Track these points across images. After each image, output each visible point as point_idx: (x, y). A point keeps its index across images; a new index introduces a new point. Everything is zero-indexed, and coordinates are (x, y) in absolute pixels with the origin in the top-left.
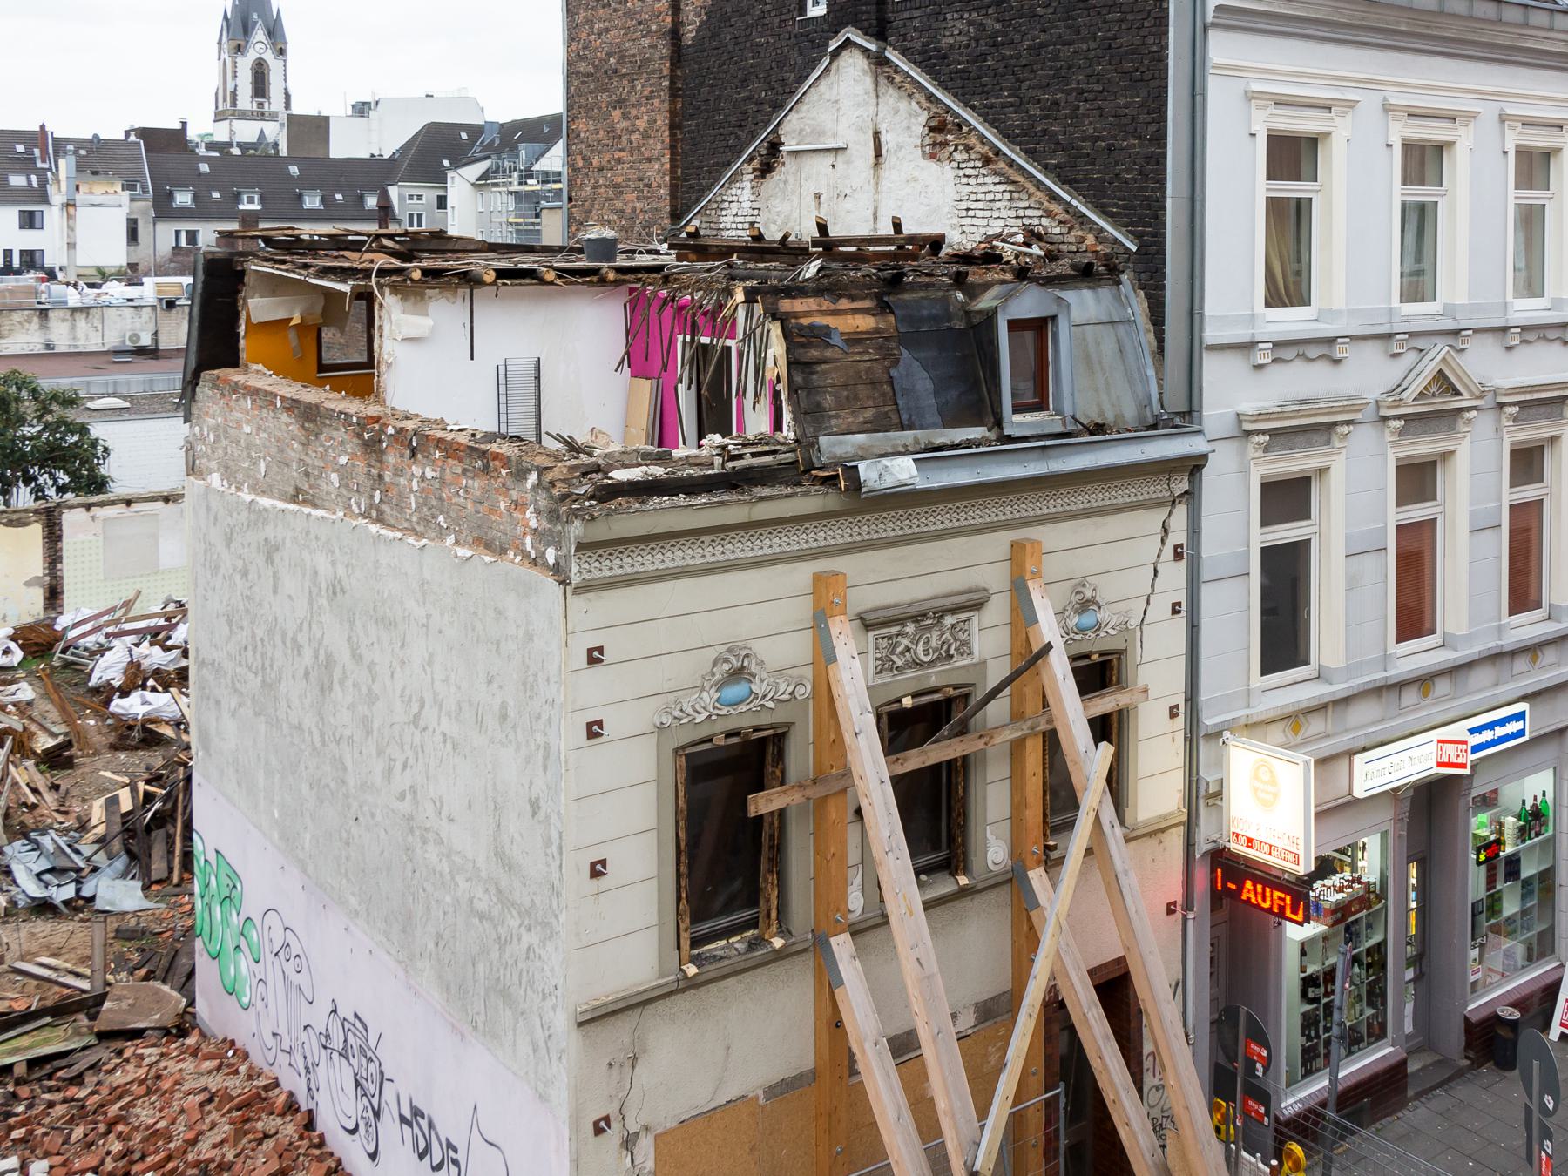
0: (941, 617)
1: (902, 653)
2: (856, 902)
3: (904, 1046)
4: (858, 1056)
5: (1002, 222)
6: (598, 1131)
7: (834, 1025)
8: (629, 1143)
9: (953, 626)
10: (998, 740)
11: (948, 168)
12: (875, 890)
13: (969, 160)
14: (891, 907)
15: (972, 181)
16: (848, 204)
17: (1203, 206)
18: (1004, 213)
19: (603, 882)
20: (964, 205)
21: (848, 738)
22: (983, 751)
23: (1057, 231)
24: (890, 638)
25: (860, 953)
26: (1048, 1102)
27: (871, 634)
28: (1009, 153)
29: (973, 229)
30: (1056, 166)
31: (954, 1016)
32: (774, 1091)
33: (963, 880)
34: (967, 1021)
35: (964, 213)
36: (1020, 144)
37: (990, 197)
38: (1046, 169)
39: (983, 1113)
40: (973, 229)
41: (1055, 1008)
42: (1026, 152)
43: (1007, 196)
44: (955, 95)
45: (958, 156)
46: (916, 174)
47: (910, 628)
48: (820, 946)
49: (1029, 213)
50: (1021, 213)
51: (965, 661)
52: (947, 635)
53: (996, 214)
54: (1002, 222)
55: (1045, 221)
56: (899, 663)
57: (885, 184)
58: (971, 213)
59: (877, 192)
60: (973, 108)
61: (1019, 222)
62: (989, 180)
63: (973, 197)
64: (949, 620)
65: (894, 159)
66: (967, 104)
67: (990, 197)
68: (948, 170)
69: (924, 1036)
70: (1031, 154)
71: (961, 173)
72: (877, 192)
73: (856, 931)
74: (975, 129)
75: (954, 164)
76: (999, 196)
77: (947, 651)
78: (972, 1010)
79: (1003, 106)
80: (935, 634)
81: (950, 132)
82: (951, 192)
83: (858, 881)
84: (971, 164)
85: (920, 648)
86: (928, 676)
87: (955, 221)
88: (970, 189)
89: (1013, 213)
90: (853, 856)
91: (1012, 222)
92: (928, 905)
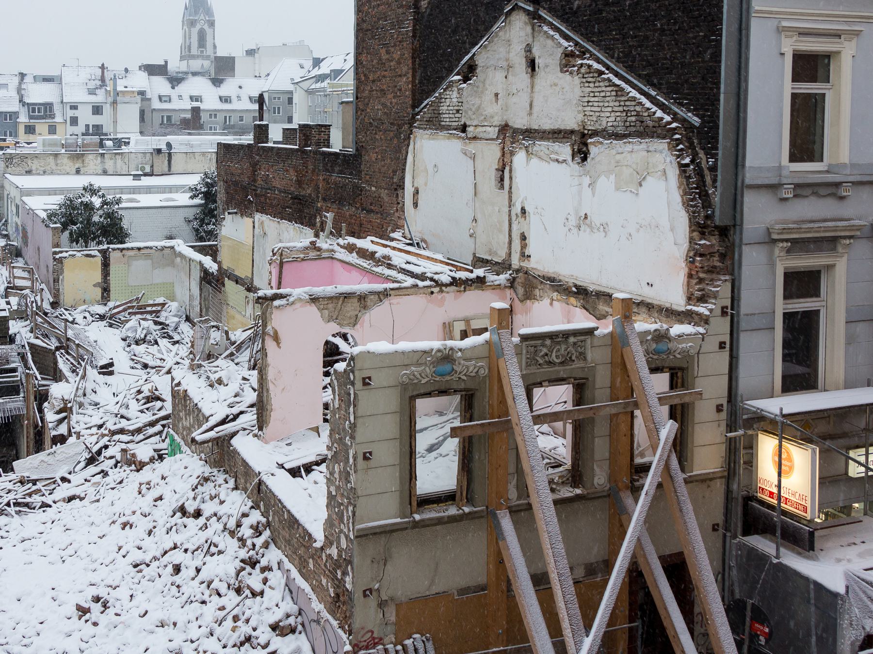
0: (567, 337)
1: (543, 356)
2: (513, 494)
3: (540, 580)
4: (512, 581)
5: (610, 109)
6: (365, 596)
7: (499, 561)
8: (382, 605)
9: (575, 344)
10: (602, 413)
11: (576, 78)
12: (523, 490)
13: (590, 73)
14: (534, 500)
15: (592, 85)
16: (514, 99)
17: (746, 98)
18: (611, 104)
19: (372, 463)
20: (586, 99)
21: (510, 401)
22: (592, 421)
23: (646, 114)
24: (535, 347)
25: (516, 524)
26: (631, 629)
27: (524, 343)
28: (615, 68)
29: (592, 113)
30: (646, 75)
31: (571, 569)
32: (462, 591)
33: (578, 491)
34: (580, 573)
35: (586, 104)
36: (622, 62)
37: (603, 94)
38: (639, 77)
39: (588, 627)
40: (592, 113)
41: (636, 576)
42: (626, 67)
43: (614, 93)
44: (582, 35)
45: (583, 70)
46: (556, 81)
47: (548, 342)
48: (490, 517)
49: (627, 103)
50: (622, 103)
51: (581, 364)
52: (571, 349)
53: (606, 104)
54: (610, 109)
55: (638, 108)
56: (541, 361)
57: (537, 88)
58: (590, 104)
59: (532, 92)
60: (593, 42)
61: (621, 109)
62: (601, 84)
63: (592, 95)
64: (572, 340)
65: (543, 73)
66: (589, 40)
67: (603, 94)
68: (577, 80)
69: (554, 577)
70: (630, 69)
71: (584, 80)
72: (532, 92)
73: (514, 512)
74: (595, 55)
75: (580, 75)
76: (608, 94)
77: (570, 358)
78: (583, 567)
79: (614, 39)
80: (563, 347)
81: (578, 56)
82: (578, 92)
83: (514, 482)
84: (591, 75)
85: (554, 354)
86: (558, 372)
87: (580, 108)
88: (590, 89)
89: (617, 104)
90: (512, 469)
91: (616, 109)
92: (556, 502)
